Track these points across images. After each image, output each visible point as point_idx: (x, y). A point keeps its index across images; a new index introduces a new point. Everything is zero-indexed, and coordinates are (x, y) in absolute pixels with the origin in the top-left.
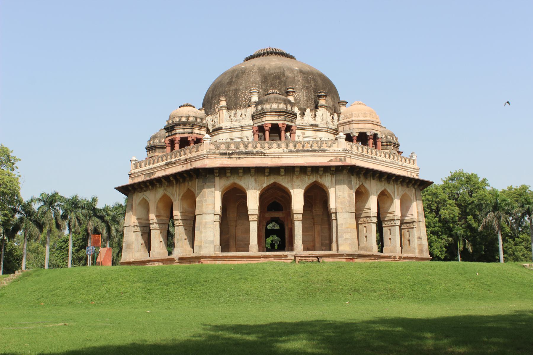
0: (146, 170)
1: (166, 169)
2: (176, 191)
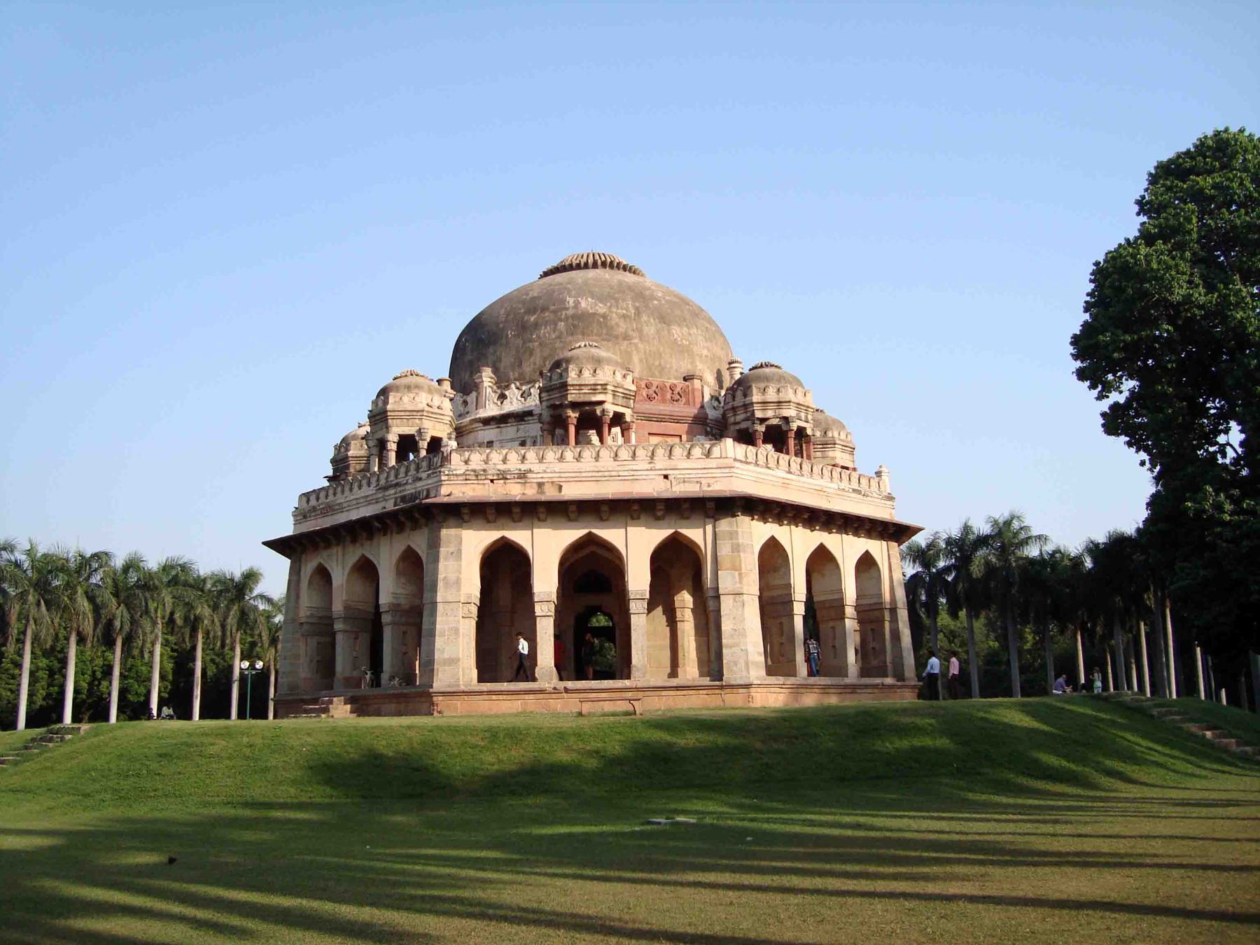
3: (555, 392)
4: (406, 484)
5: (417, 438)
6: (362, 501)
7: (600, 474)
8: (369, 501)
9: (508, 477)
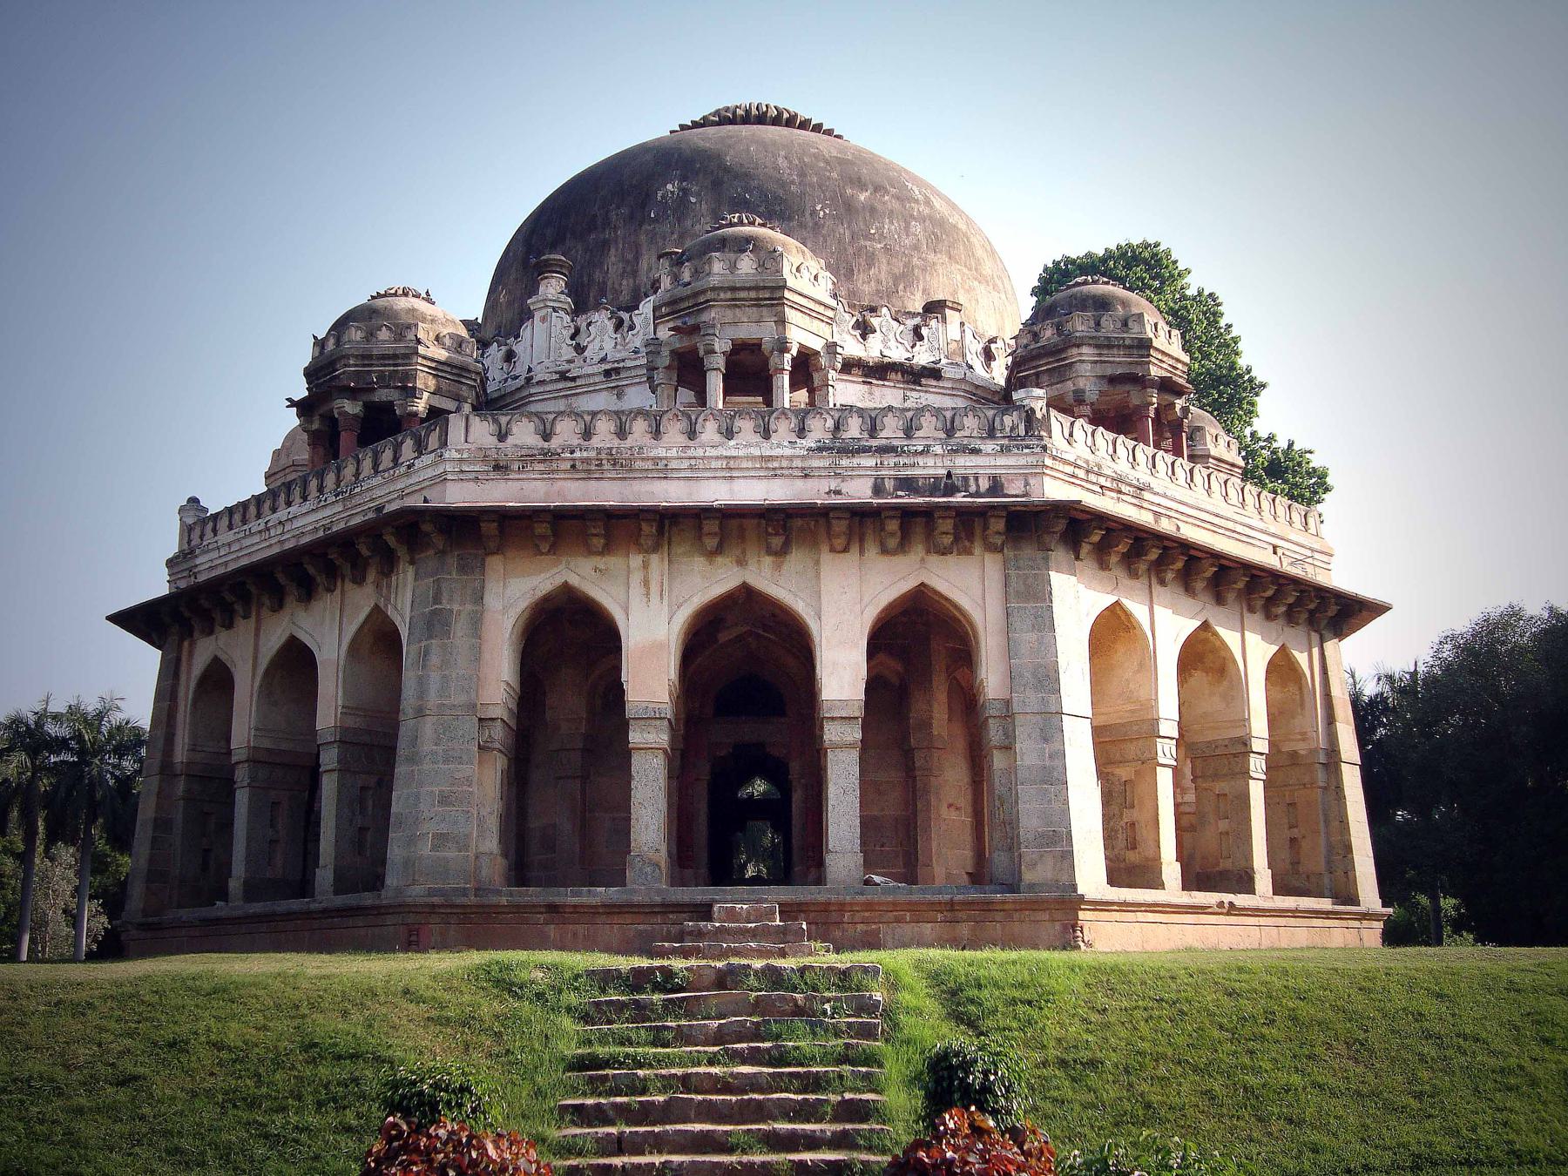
3: (1115, 351)
4: (926, 452)
5: (823, 361)
6: (744, 465)
7: (1216, 520)
8: (770, 468)
9: (1124, 488)
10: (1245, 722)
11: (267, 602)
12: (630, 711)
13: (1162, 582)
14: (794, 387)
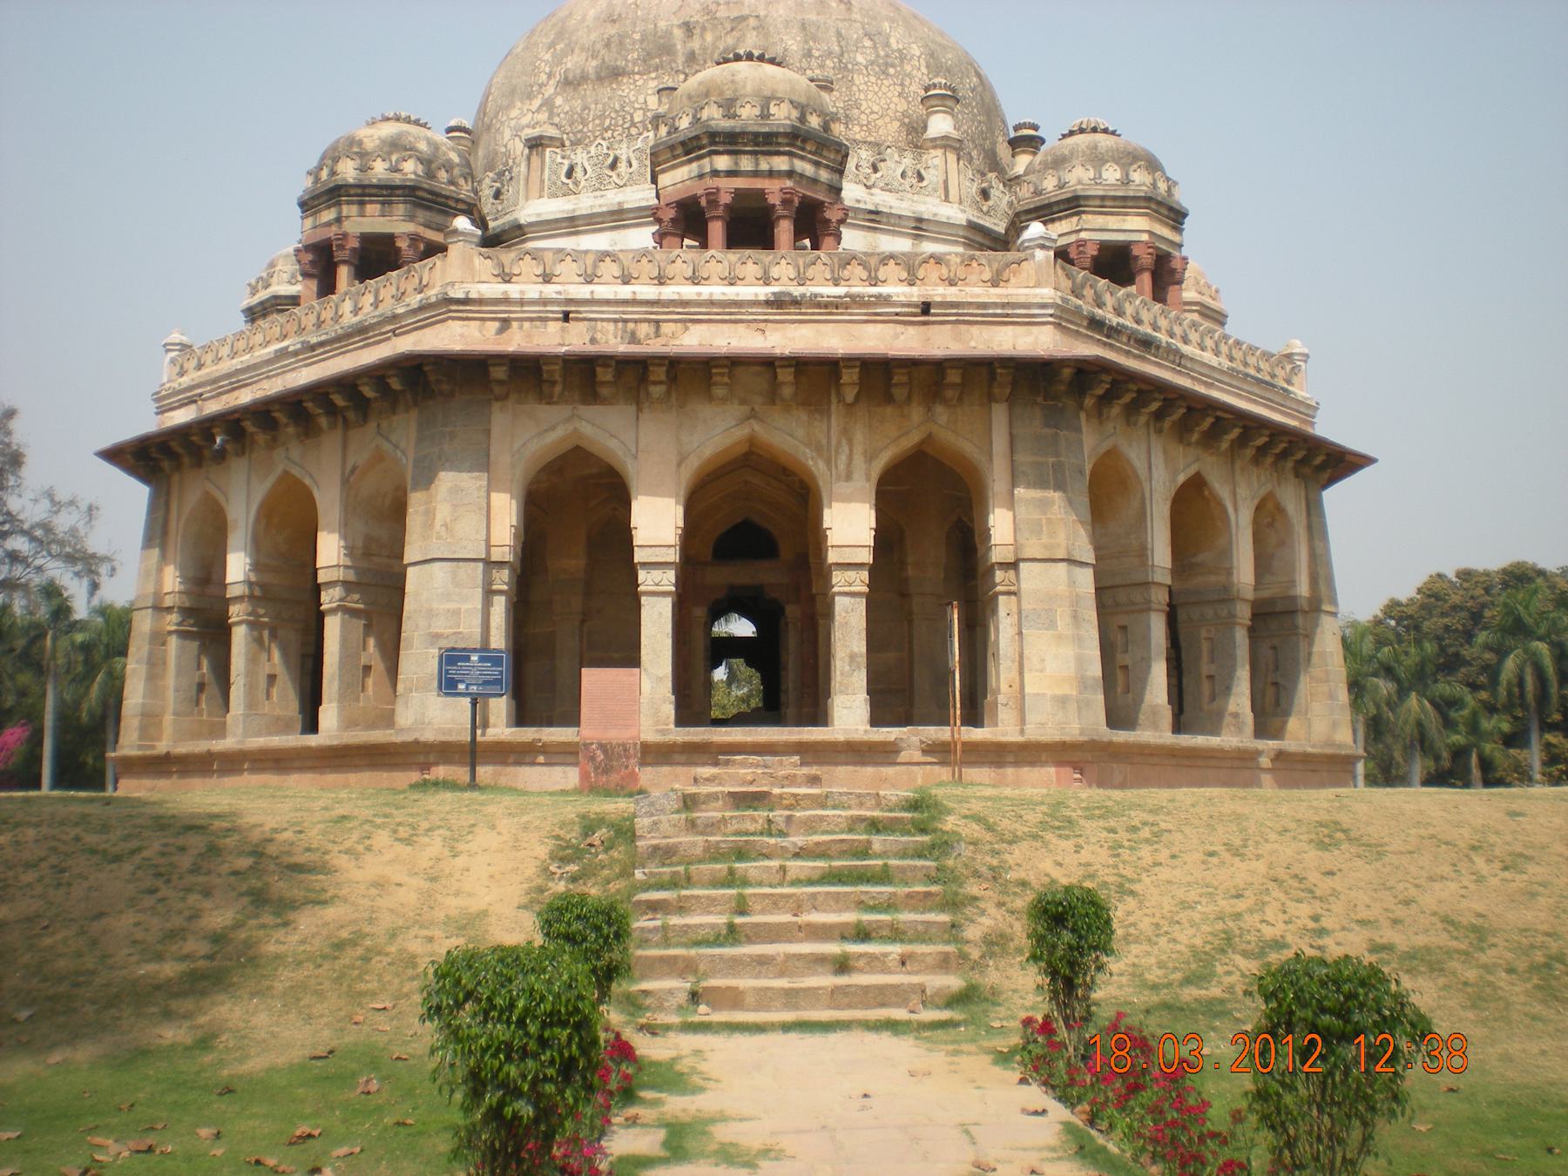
0: (608, 302)
1: (766, 321)
2: (846, 432)
10: (1229, 572)
11: (261, 438)
12: (639, 556)
13: (1159, 431)
14: (798, 234)
